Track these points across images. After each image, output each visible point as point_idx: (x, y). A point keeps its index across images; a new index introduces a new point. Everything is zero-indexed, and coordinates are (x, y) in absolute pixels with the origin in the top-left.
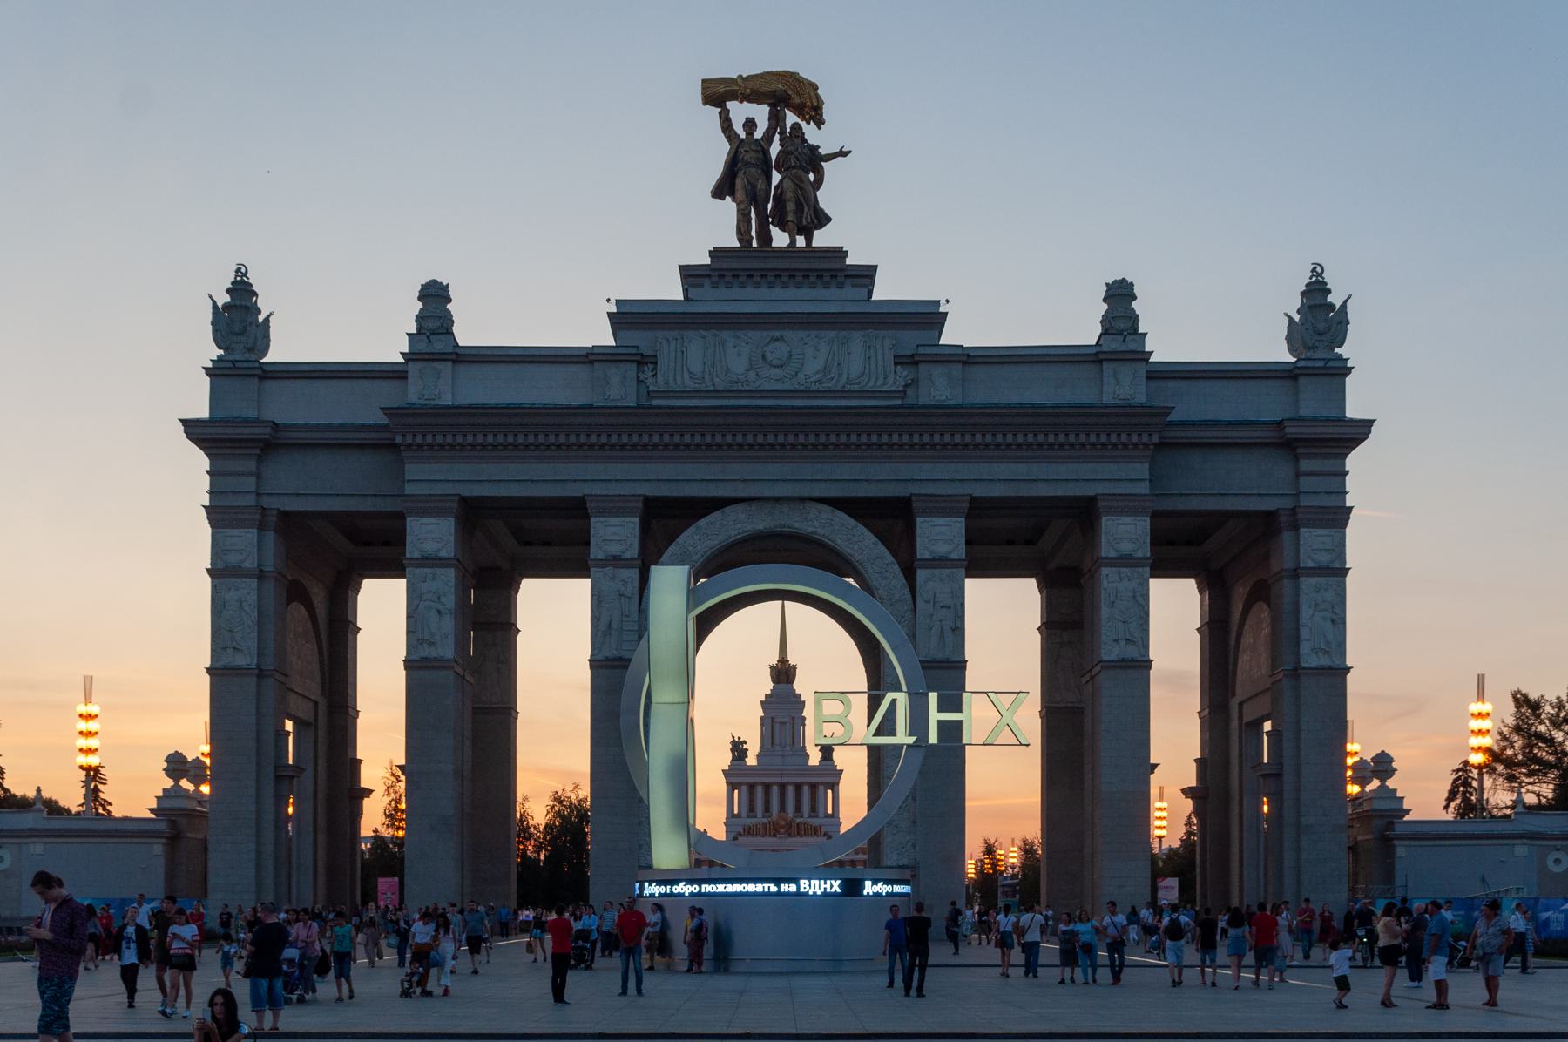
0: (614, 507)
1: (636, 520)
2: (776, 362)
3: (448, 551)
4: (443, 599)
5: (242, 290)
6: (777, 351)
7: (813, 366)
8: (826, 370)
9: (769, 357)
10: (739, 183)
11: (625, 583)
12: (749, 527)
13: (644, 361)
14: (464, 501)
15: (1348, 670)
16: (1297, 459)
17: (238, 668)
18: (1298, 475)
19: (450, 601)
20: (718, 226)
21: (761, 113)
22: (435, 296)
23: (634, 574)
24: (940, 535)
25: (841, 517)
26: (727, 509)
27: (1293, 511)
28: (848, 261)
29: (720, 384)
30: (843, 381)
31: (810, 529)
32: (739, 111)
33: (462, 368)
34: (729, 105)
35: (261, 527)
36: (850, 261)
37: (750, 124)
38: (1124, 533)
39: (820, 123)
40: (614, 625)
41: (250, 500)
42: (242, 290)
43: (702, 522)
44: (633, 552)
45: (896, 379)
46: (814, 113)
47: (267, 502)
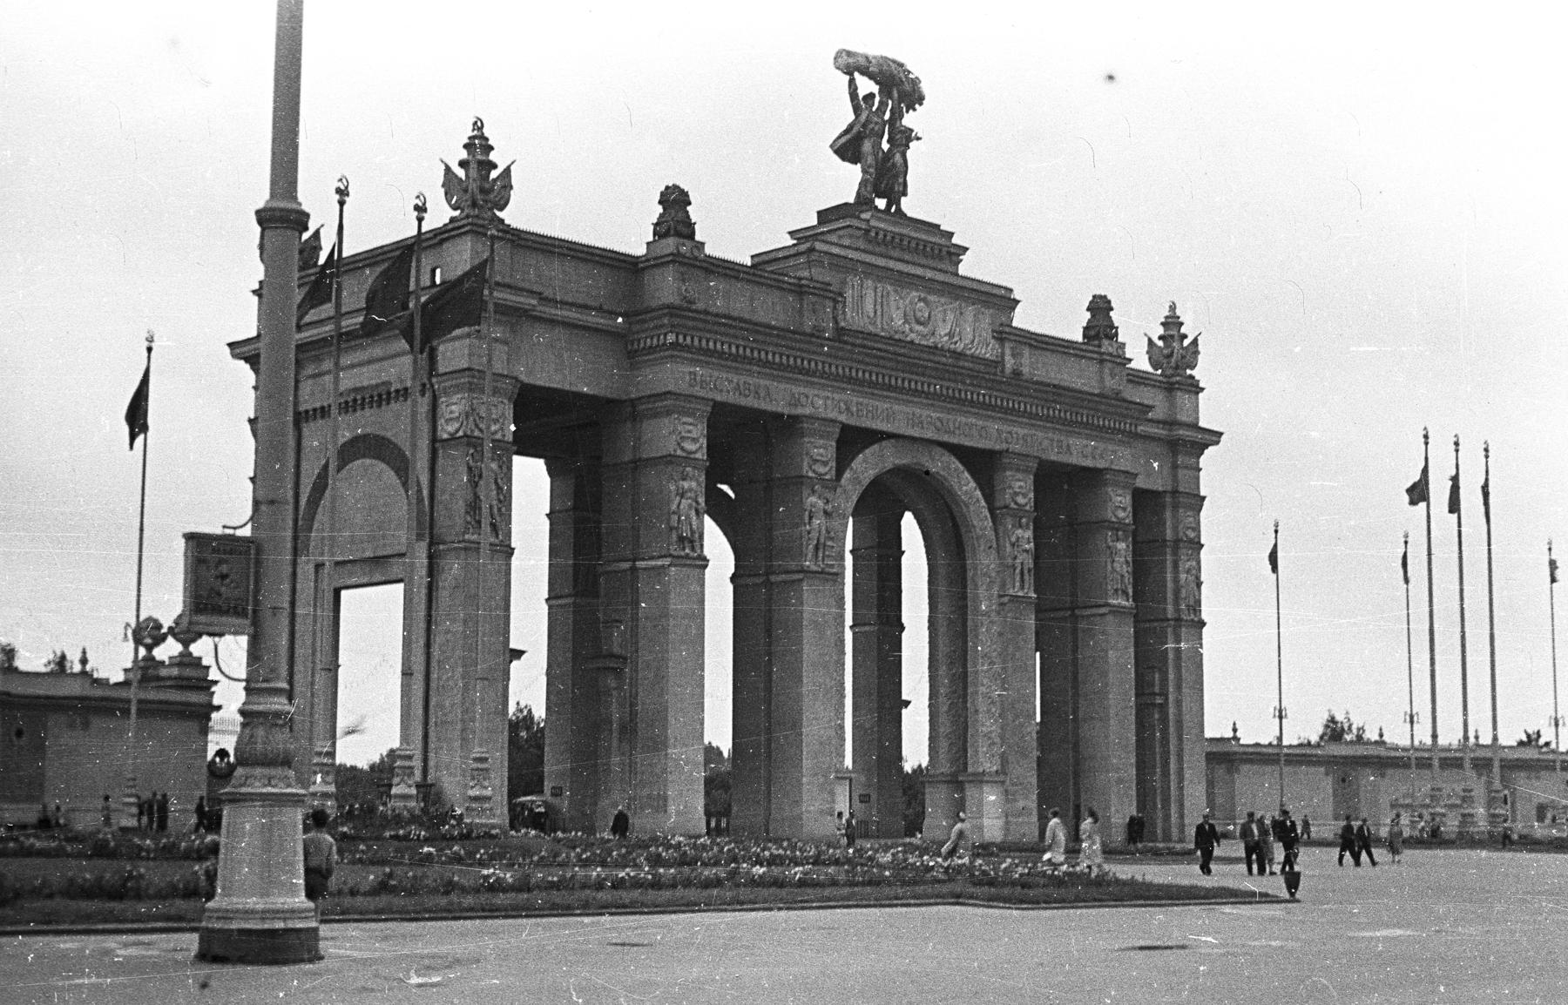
5: (479, 145)
7: (943, 330)
8: (951, 335)
9: (919, 314)
10: (867, 146)
15: (1203, 624)
16: (1175, 454)
18: (1175, 467)
20: (845, 182)
21: (873, 87)
22: (675, 200)
24: (1019, 488)
25: (956, 464)
27: (1175, 492)
28: (954, 240)
32: (866, 86)
34: (856, 75)
36: (954, 240)
37: (870, 96)
38: (1119, 504)
39: (911, 107)
42: (479, 145)
45: (989, 351)
46: (913, 97)
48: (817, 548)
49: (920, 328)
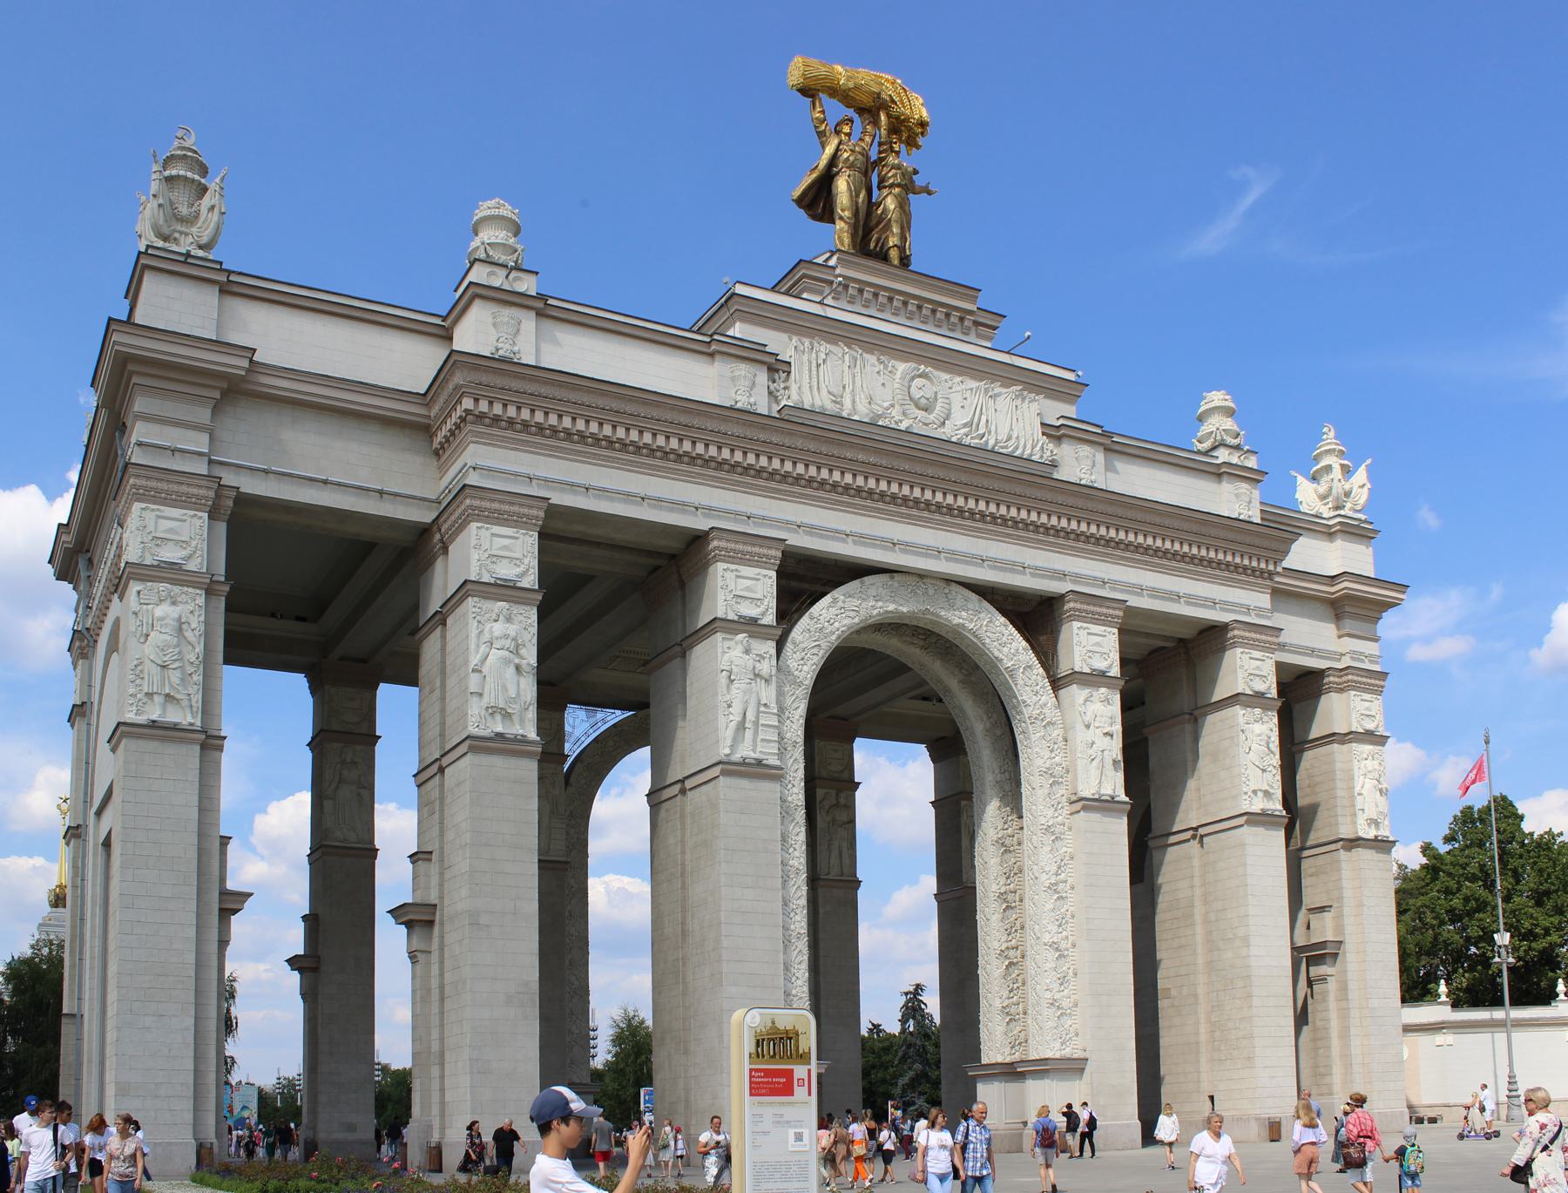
0: (747, 546)
1: (774, 574)
2: (923, 401)
3: (530, 580)
4: (523, 652)
6: (920, 389)
7: (959, 418)
9: (916, 394)
11: (761, 657)
12: (891, 607)
13: (776, 367)
14: (554, 512)
17: (175, 728)
19: (530, 656)
23: (770, 647)
26: (868, 580)
29: (862, 412)
30: (991, 442)
31: (956, 621)
33: (548, 325)
35: (213, 515)
40: (750, 716)
41: (202, 468)
43: (838, 593)
44: (770, 619)
47: (229, 479)
48: (741, 726)
49: (920, 414)
